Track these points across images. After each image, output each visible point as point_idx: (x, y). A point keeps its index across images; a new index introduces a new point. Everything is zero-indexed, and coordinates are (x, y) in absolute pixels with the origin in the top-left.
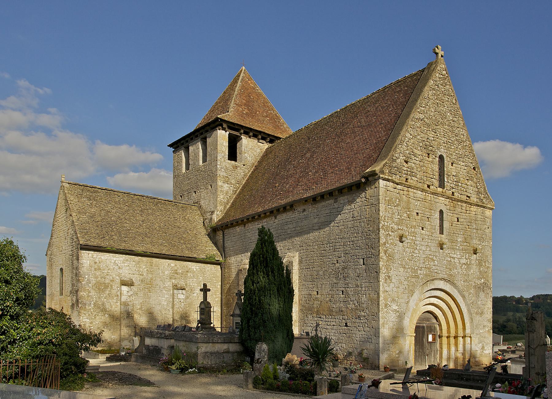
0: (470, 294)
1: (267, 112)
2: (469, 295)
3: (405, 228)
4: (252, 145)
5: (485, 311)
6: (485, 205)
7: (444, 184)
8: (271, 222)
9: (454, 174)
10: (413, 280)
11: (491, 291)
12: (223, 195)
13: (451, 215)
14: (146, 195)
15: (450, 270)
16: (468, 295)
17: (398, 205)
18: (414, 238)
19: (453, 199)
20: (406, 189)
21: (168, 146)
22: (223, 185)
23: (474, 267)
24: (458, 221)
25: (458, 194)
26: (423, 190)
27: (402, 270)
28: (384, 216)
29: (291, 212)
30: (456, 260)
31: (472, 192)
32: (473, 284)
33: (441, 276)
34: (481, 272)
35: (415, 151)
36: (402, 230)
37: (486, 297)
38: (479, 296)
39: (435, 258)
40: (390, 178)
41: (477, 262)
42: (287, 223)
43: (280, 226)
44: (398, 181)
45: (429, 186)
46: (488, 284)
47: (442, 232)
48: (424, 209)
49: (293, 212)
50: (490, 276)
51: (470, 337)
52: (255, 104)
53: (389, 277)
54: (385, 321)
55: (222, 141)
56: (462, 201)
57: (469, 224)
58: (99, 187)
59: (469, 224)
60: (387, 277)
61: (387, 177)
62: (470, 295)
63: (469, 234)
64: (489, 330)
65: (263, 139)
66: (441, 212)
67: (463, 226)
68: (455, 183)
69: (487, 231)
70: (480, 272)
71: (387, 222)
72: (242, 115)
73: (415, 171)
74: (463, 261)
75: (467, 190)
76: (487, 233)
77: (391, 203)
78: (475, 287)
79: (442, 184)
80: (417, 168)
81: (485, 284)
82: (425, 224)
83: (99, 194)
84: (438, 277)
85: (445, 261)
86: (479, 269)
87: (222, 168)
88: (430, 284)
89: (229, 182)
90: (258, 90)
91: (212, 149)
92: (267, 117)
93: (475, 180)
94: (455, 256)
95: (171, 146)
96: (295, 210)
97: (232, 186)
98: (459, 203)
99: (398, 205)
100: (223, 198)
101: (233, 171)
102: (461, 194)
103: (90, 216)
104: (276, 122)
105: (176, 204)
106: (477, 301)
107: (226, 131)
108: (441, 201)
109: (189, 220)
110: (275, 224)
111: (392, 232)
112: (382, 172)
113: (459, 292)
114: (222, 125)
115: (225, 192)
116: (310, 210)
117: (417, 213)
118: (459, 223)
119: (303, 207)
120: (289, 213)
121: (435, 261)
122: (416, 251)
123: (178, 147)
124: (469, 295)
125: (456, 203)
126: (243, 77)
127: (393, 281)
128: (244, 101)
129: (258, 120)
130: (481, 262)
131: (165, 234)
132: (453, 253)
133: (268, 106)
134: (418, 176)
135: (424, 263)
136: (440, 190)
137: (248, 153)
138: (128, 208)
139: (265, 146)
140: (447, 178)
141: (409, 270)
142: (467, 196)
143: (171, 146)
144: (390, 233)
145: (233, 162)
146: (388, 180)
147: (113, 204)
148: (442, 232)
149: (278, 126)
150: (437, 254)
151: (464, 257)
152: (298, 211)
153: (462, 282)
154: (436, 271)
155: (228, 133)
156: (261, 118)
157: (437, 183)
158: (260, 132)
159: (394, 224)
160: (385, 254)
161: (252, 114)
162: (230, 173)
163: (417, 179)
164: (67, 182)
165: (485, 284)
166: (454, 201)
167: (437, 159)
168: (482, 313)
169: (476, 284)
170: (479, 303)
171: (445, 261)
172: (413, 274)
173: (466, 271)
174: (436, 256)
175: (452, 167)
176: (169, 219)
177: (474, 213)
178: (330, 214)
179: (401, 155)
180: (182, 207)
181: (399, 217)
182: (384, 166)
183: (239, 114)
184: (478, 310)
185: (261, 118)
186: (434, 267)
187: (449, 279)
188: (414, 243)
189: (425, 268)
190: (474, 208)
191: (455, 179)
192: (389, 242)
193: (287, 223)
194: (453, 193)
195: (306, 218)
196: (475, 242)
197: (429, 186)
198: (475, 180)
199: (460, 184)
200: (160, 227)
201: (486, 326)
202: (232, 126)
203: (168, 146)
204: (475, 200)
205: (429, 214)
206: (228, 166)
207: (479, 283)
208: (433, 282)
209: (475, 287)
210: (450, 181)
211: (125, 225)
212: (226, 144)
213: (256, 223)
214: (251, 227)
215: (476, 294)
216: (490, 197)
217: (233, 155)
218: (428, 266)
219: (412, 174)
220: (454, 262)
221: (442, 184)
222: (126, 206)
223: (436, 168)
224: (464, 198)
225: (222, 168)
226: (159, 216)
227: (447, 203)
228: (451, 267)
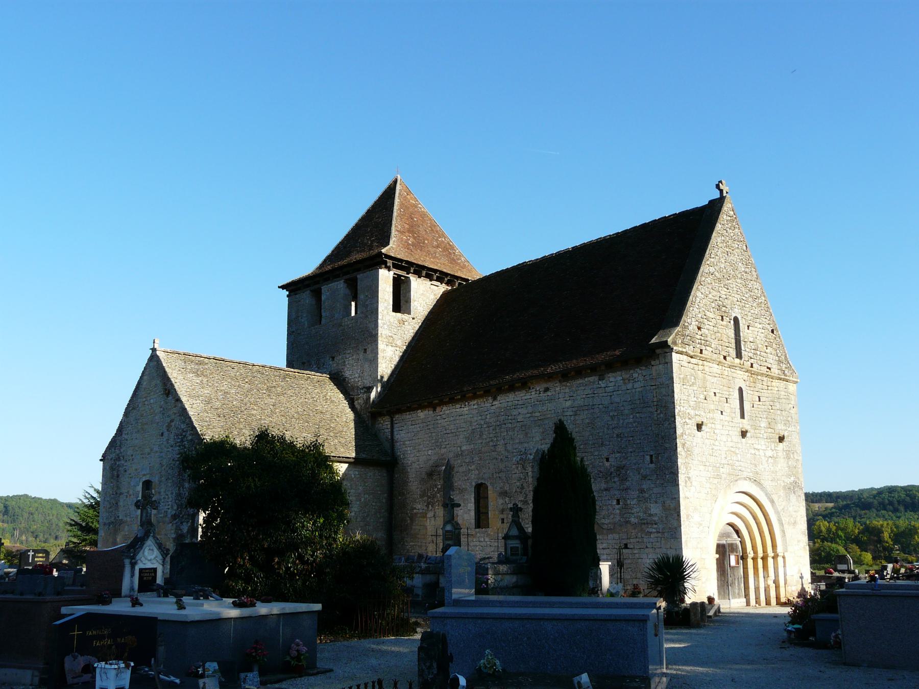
0: (779, 497)
1: (437, 240)
2: (778, 499)
3: (702, 413)
4: (424, 289)
6: (788, 378)
7: (741, 353)
8: (486, 405)
9: (751, 339)
10: (716, 481)
12: (386, 362)
13: (752, 393)
14: (269, 365)
15: (756, 466)
17: (693, 384)
18: (713, 425)
19: (753, 372)
20: (701, 362)
21: (279, 287)
22: (385, 348)
23: (782, 460)
24: (760, 401)
25: (757, 365)
26: (719, 363)
27: (702, 468)
28: (679, 399)
29: (524, 391)
30: (762, 453)
31: (772, 362)
32: (783, 484)
33: (745, 474)
34: (789, 467)
35: (708, 313)
36: (699, 416)
38: (789, 499)
39: (737, 451)
40: (684, 350)
41: (784, 453)
42: (516, 407)
43: (502, 410)
44: (692, 354)
45: (725, 358)
47: (743, 416)
48: (721, 387)
49: (526, 391)
51: (784, 557)
52: (421, 229)
53: (689, 478)
54: (687, 538)
55: (385, 284)
56: (762, 374)
57: (771, 403)
58: (205, 355)
59: (771, 403)
60: (687, 479)
61: (681, 349)
63: (773, 417)
65: (438, 279)
66: (741, 390)
67: (765, 406)
68: (752, 351)
69: (793, 412)
70: (789, 467)
71: (684, 407)
72: (407, 246)
73: (708, 339)
74: (769, 453)
75: (767, 359)
76: (793, 415)
77: (686, 381)
78: (784, 487)
79: (739, 355)
80: (711, 335)
82: (724, 407)
83: (206, 367)
85: (749, 455)
86: (788, 463)
87: (384, 324)
88: (734, 485)
89: (394, 344)
90: (421, 208)
91: (367, 296)
92: (438, 247)
93: (774, 346)
94: (759, 447)
95: (283, 287)
96: (530, 388)
97: (398, 349)
98: (759, 377)
99: (693, 384)
100: (386, 368)
101: (399, 328)
102: (761, 365)
103: (206, 401)
104: (450, 253)
105: (309, 377)
107: (389, 270)
108: (739, 375)
109: (332, 402)
110: (493, 407)
111: (689, 419)
112: (675, 343)
113: (766, 495)
114: (385, 263)
115: (388, 358)
116: (558, 389)
117: (715, 393)
118: (761, 403)
119: (545, 385)
120: (520, 393)
121: (738, 455)
122: (717, 443)
123: (299, 289)
124: (778, 499)
125: (756, 377)
126: (400, 190)
127: (694, 483)
128: (407, 226)
129: (428, 253)
130: (788, 454)
131: (307, 424)
132: (757, 442)
133: (437, 231)
134: (713, 346)
135: (726, 458)
136: (737, 361)
137: (418, 301)
138: (249, 386)
139: (441, 289)
140: (745, 345)
141: (710, 468)
142: (768, 368)
143: (283, 287)
144: (687, 421)
145: (399, 315)
146: (681, 353)
147: (229, 380)
148: (743, 416)
149: (454, 260)
150: (740, 445)
151: (770, 448)
152: (536, 391)
153: (770, 482)
154: (740, 468)
155: (392, 273)
156: (432, 250)
157: (733, 353)
158: (435, 271)
159: (690, 409)
160: (684, 448)
161: (419, 244)
162: (395, 330)
163: (712, 349)
164: (163, 349)
167: (732, 322)
168: (795, 523)
169: (786, 484)
171: (749, 455)
172: (715, 474)
173: (773, 466)
174: (739, 449)
175: (748, 331)
176: (306, 400)
177: (776, 389)
178: (593, 395)
179: (693, 319)
180: (318, 381)
181: (695, 399)
182: (676, 335)
183: (402, 244)
185: (432, 250)
186: (737, 462)
187: (755, 479)
188: (714, 433)
189: (728, 464)
190: (776, 383)
191: (753, 347)
192: (687, 433)
193: (516, 407)
194: (752, 364)
195: (551, 400)
196: (781, 429)
197: (725, 358)
198: (774, 346)
199: (758, 353)
200: (297, 413)
202: (399, 264)
203: (279, 287)
204: (777, 372)
205: (727, 393)
206: (392, 320)
208: (736, 483)
209: (784, 487)
210: (747, 350)
211: (254, 412)
212: (390, 289)
213: (458, 406)
214: (448, 412)
215: (787, 497)
216: (793, 367)
217: (400, 303)
218: (731, 461)
219: (707, 343)
220: (759, 455)
221: (739, 355)
222: (247, 382)
223: (731, 333)
224: (764, 370)
225: (384, 324)
226: (292, 396)
227: (745, 378)
228: (756, 462)
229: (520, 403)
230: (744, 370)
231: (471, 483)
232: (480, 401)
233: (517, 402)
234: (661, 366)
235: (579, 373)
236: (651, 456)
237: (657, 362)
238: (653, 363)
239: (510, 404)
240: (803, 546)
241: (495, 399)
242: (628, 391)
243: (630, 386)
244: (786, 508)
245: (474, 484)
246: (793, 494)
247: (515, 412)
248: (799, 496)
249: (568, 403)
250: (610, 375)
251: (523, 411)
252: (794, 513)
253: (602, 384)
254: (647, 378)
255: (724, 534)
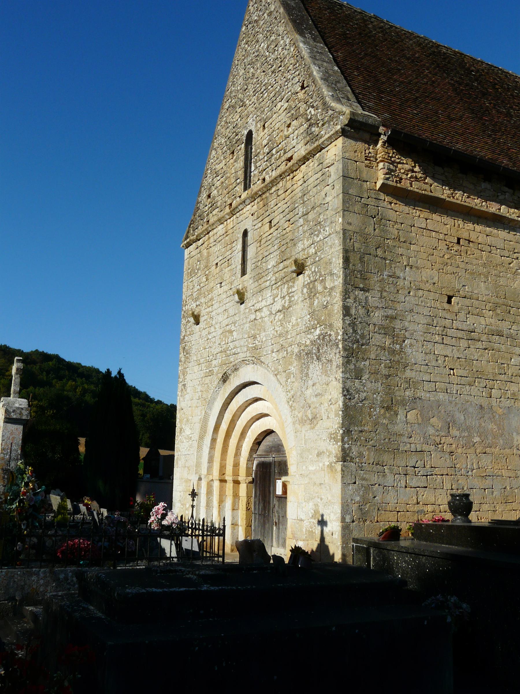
5: (323, 412)
11: (338, 351)
16: (284, 379)
19: (260, 193)
23: (300, 305)
32: (296, 350)
37: (326, 371)
38: (307, 375)
46: (330, 335)
50: (336, 311)
54: (179, 455)
62: (289, 380)
64: (331, 464)
78: (299, 356)
81: (324, 338)
84: (236, 362)
106: (303, 390)
148: (244, 272)
154: (233, 351)
165: (324, 338)
166: (263, 193)
168: (314, 420)
170: (309, 392)
184: (306, 412)
201: (323, 452)
207: (308, 342)
209: (299, 356)
215: (302, 372)
230: (248, 202)
240: (327, 463)
244: (299, 393)
246: (316, 363)
248: (330, 361)
252: (314, 399)
255: (273, 447)
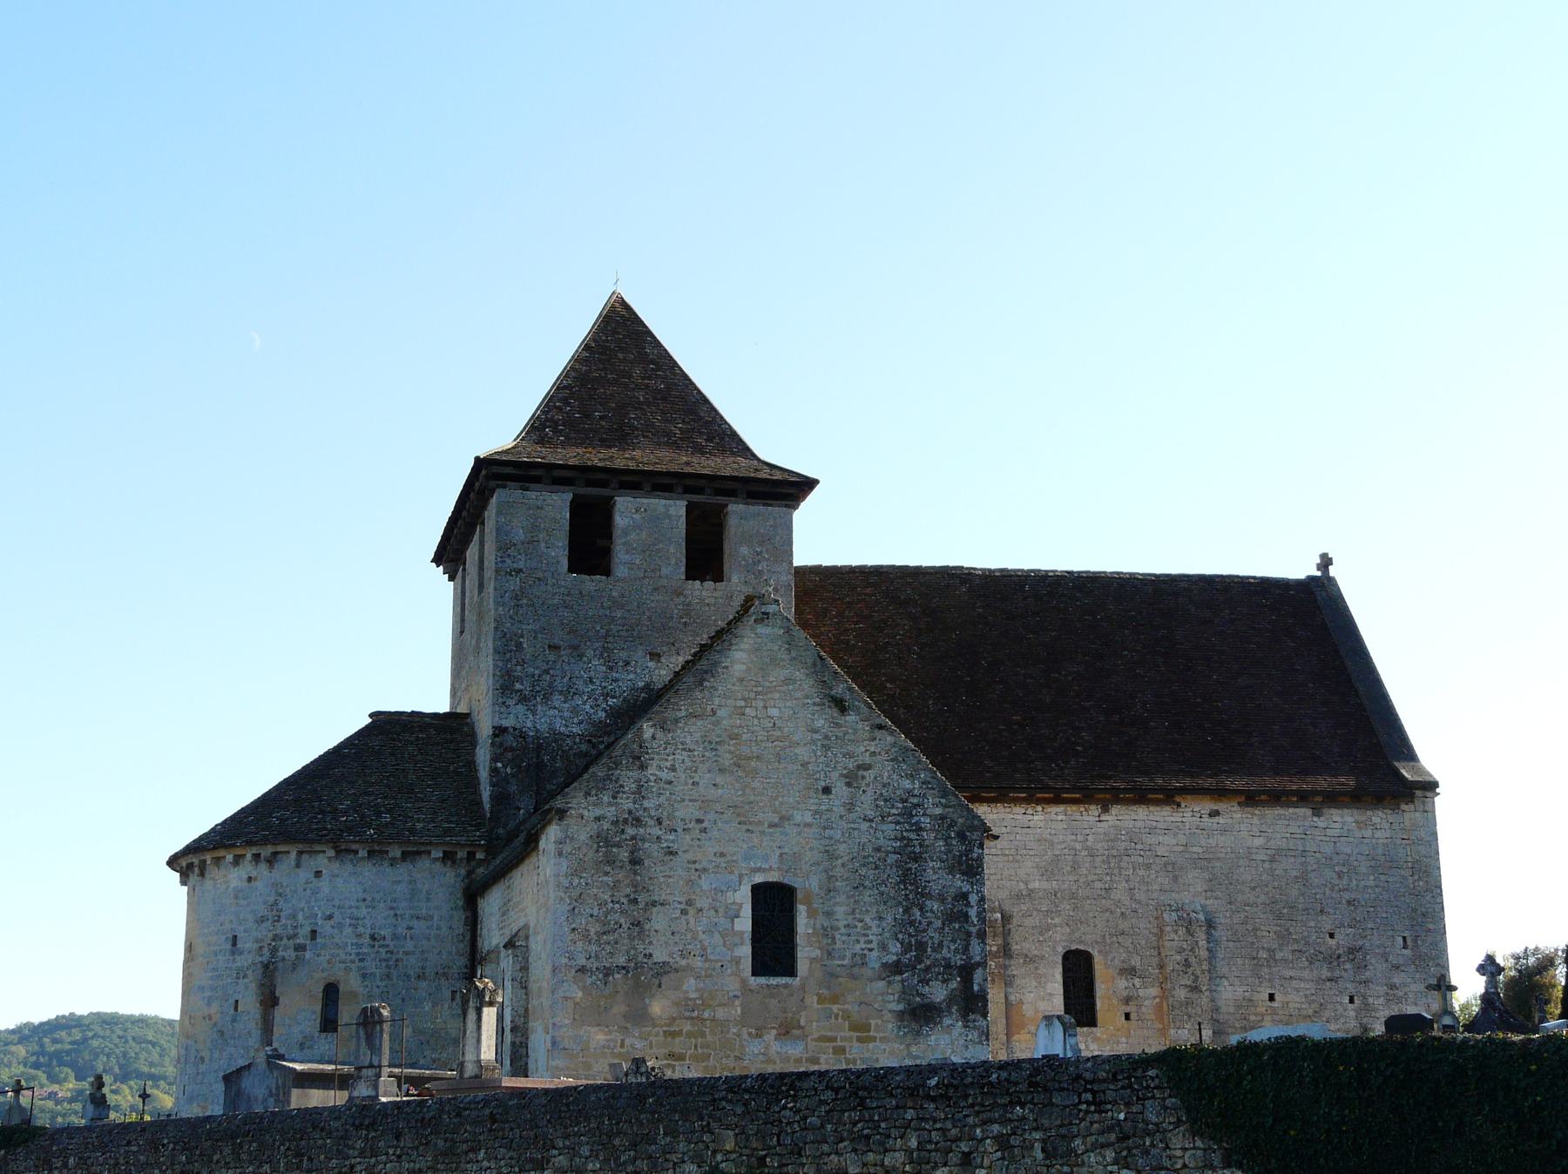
8: (1086, 818)
29: (1168, 808)
42: (1152, 831)
43: (1123, 833)
120: (1158, 809)
178: (1304, 836)
193: (1152, 831)
195: (1224, 831)
229: (1161, 825)
231: (1054, 949)
232: (1071, 809)
233: (1154, 824)
234: (1417, 814)
235: (1277, 798)
236: (1404, 938)
237: (1411, 807)
238: (1403, 807)
239: (1138, 824)
241: (1105, 810)
242: (1366, 841)
243: (1368, 833)
245: (1061, 950)
247: (1152, 840)
249: (1259, 842)
250: (1333, 811)
251: (1169, 840)
253: (1320, 822)
254: (1396, 826)
